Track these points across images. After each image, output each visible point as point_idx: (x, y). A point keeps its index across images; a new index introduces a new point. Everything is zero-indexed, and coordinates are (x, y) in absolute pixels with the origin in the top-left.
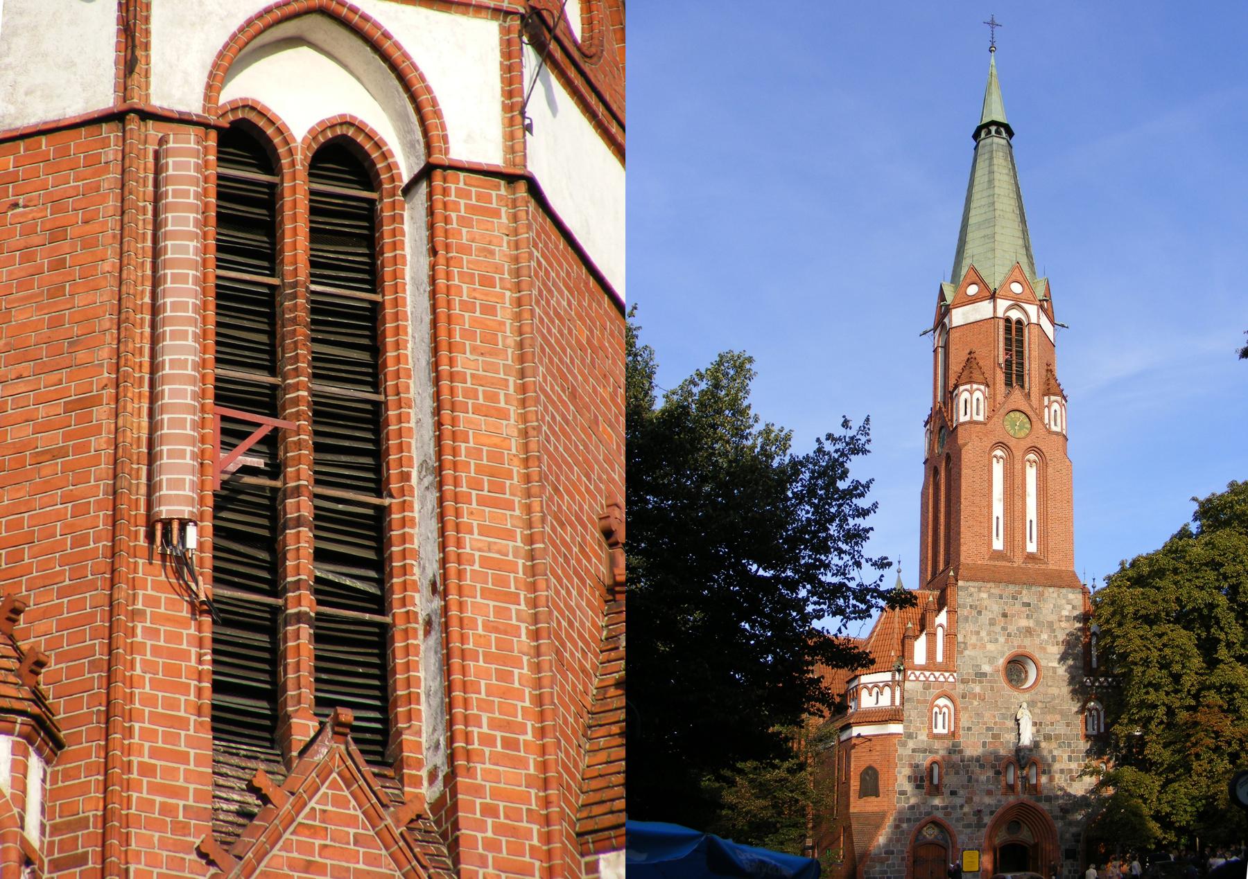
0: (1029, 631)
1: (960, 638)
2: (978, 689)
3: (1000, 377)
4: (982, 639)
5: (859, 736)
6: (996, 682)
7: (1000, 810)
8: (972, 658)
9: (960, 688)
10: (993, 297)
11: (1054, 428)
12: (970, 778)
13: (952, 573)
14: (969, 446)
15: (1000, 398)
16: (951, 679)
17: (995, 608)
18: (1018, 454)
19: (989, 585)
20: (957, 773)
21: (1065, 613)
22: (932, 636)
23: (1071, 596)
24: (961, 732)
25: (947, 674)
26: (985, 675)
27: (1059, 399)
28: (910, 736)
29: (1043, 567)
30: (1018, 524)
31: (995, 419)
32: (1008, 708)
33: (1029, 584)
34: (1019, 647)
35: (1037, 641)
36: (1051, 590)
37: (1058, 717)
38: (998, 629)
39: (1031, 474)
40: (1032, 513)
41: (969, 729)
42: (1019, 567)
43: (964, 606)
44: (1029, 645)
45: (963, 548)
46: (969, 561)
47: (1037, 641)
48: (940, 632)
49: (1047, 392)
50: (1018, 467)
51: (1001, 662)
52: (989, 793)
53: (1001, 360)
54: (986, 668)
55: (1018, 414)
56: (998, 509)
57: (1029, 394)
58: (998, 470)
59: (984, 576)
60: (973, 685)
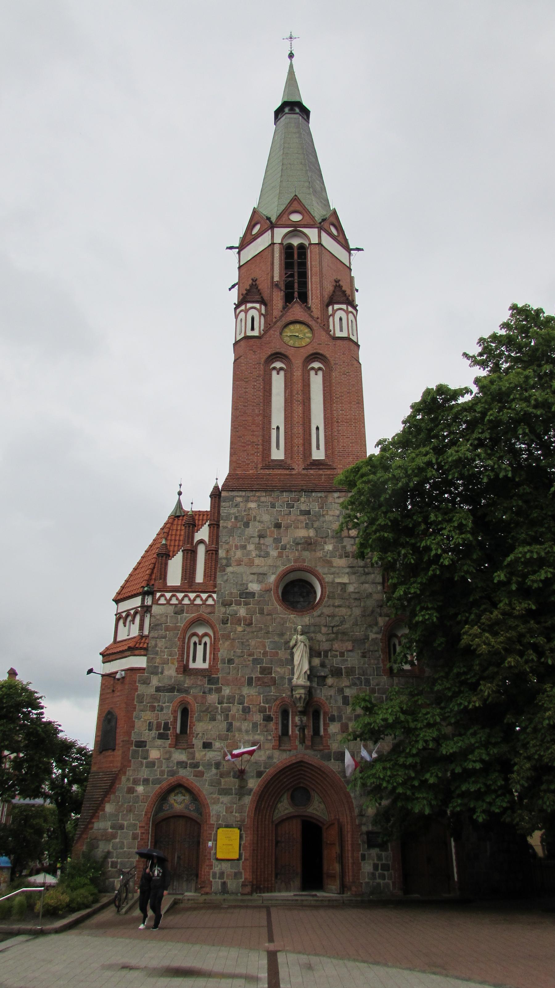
1: (222, 553)
2: (242, 612)
7: (270, 772)
9: (221, 611)
11: (338, 334)
12: (230, 727)
15: (276, 313)
19: (258, 494)
20: (213, 719)
24: (220, 666)
25: (204, 596)
26: (252, 594)
27: (344, 307)
31: (271, 332)
32: (282, 635)
35: (320, 554)
37: (349, 645)
38: (269, 541)
39: (317, 383)
41: (230, 661)
42: (299, 474)
43: (228, 518)
44: (309, 558)
47: (320, 554)
48: (201, 551)
50: (298, 374)
51: (272, 579)
54: (254, 587)
55: (298, 326)
56: (278, 418)
58: (278, 382)
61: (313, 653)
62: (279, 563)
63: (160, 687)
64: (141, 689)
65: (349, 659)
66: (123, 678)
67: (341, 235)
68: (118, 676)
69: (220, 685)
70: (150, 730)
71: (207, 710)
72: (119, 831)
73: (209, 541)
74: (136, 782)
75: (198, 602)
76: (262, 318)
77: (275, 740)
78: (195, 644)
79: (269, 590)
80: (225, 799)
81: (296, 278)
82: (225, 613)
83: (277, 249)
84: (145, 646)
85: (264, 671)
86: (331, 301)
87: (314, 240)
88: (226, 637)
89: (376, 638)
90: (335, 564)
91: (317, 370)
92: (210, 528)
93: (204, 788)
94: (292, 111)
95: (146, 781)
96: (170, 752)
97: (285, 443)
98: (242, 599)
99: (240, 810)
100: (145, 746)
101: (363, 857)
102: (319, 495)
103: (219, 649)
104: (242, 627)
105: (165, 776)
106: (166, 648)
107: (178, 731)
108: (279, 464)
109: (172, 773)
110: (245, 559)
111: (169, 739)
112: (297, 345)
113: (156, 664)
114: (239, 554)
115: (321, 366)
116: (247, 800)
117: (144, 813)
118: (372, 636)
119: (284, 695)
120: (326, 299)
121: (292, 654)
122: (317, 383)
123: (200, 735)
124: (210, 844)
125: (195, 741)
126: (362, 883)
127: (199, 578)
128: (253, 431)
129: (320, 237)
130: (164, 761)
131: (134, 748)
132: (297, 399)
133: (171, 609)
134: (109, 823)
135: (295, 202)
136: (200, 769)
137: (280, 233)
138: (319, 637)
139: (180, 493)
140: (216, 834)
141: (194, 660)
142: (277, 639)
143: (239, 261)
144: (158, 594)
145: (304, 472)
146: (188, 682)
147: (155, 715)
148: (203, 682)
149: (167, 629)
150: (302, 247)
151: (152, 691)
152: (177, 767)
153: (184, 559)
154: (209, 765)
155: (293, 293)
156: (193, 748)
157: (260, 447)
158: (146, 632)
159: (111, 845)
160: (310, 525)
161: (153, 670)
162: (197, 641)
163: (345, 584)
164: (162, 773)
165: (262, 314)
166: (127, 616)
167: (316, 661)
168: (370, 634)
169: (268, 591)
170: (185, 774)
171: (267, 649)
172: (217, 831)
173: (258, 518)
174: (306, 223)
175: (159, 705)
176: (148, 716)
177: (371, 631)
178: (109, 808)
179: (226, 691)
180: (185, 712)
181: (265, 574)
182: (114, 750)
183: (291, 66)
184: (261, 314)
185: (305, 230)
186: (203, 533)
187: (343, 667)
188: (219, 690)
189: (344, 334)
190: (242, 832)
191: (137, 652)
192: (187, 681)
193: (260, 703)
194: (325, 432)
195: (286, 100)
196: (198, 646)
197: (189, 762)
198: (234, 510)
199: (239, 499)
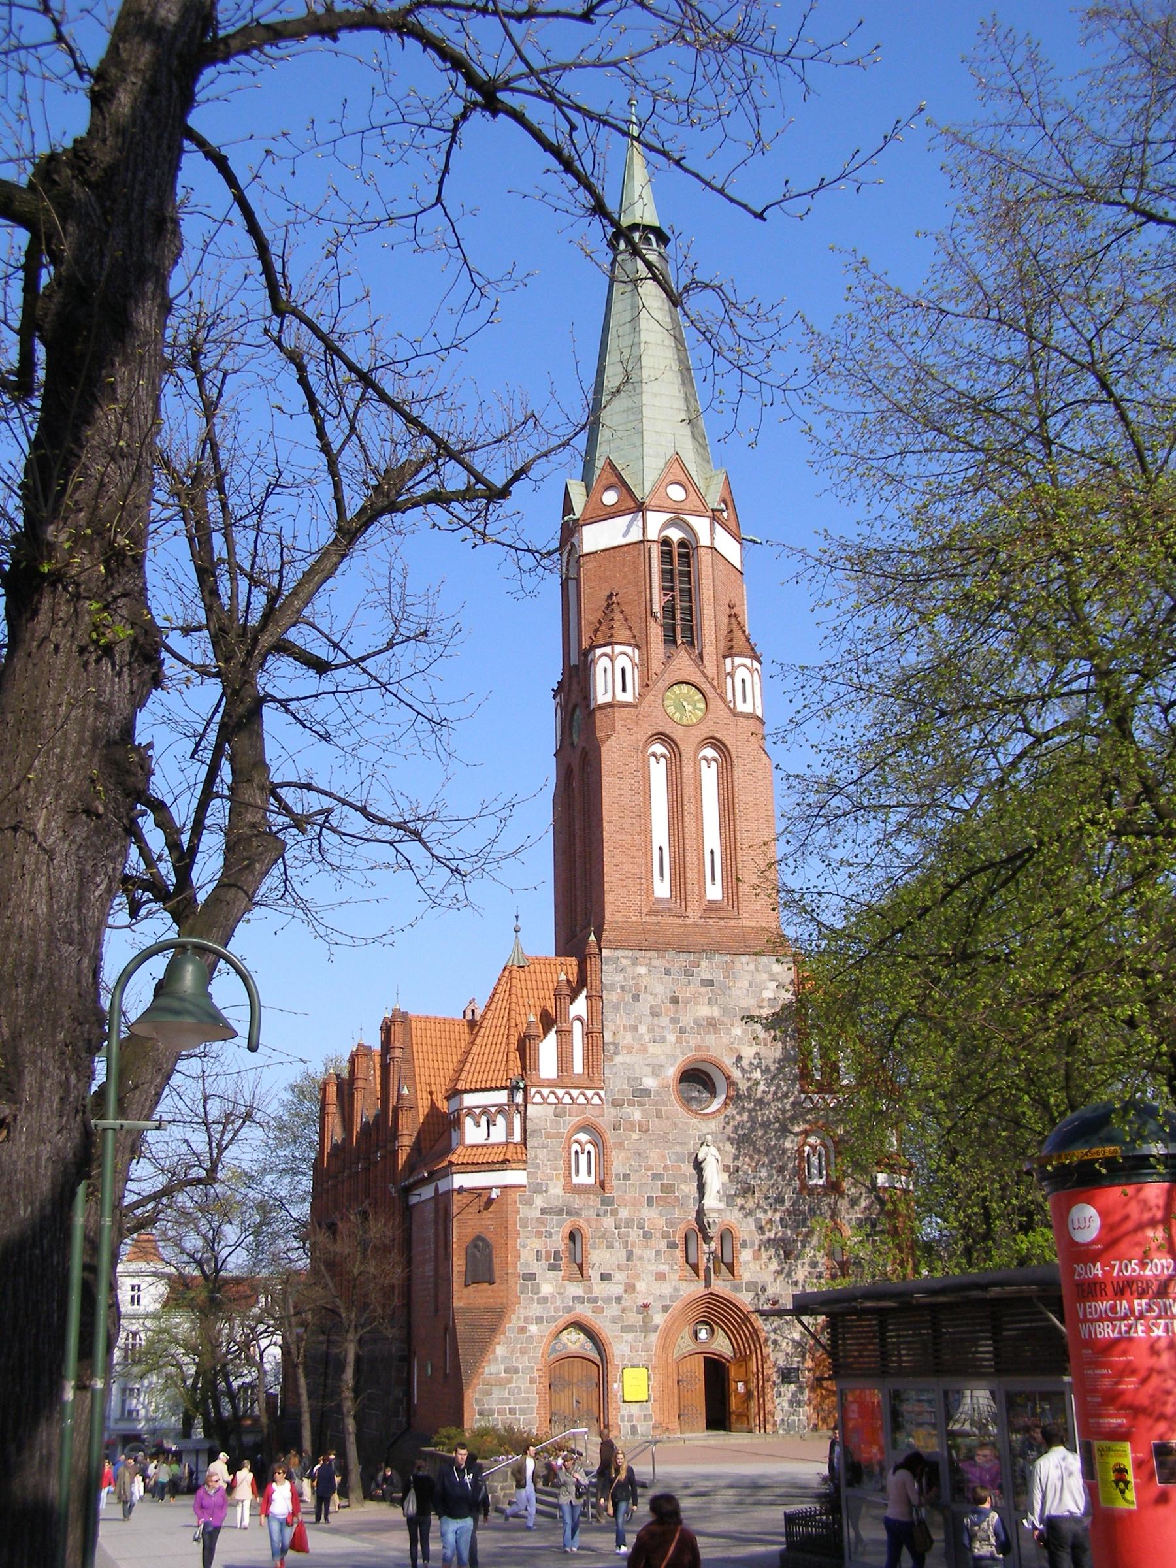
0: (712, 1025)
1: (608, 1037)
2: (637, 1115)
3: (656, 632)
5: (461, 1190)
6: (664, 1103)
7: (677, 1304)
8: (629, 1067)
9: (611, 1113)
10: (640, 508)
11: (741, 708)
13: (592, 938)
14: (612, 742)
15: (656, 666)
16: (596, 1100)
17: (661, 989)
18: (687, 749)
19: (649, 954)
20: (610, 1246)
21: (768, 994)
22: (564, 1036)
23: (777, 968)
24: (614, 1182)
25: (589, 1093)
26: (647, 1092)
27: (747, 661)
28: (538, 1189)
29: (732, 923)
30: (691, 858)
31: (650, 698)
33: (711, 949)
34: (698, 1048)
36: (744, 959)
38: (664, 1021)
39: (710, 777)
40: (712, 839)
41: (626, 1177)
43: (613, 987)
45: (608, 898)
46: (619, 918)
47: (726, 1039)
48: (577, 1028)
49: (729, 653)
50: (688, 769)
51: (672, 1072)
52: (661, 1277)
53: (657, 608)
54: (649, 1083)
55: (685, 688)
57: (701, 655)
59: (644, 942)
60: (629, 1110)
62: (678, 1052)
64: (524, 1211)
71: (603, 1236)
75: (582, 1100)
79: (668, 1087)
80: (630, 1337)
85: (667, 1188)
88: (620, 1145)
93: (604, 1326)
95: (539, 1320)
96: (564, 1287)
99: (647, 1349)
109: (568, 1310)
110: (637, 1045)
112: (685, 722)
114: (627, 1039)
125: (591, 1272)
127: (578, 1067)
134: (502, 1367)
142: (678, 1149)
144: (533, 1091)
146: (577, 1202)
148: (595, 1201)
150: (682, 544)
151: (538, 1214)
153: (560, 1044)
154: (608, 1300)
164: (556, 1310)
170: (584, 1312)
176: (536, 1244)
178: (500, 1350)
179: (624, 1213)
180: (572, 1237)
184: (634, 665)
188: (614, 1213)
191: (514, 1165)
198: (619, 978)
199: (624, 961)
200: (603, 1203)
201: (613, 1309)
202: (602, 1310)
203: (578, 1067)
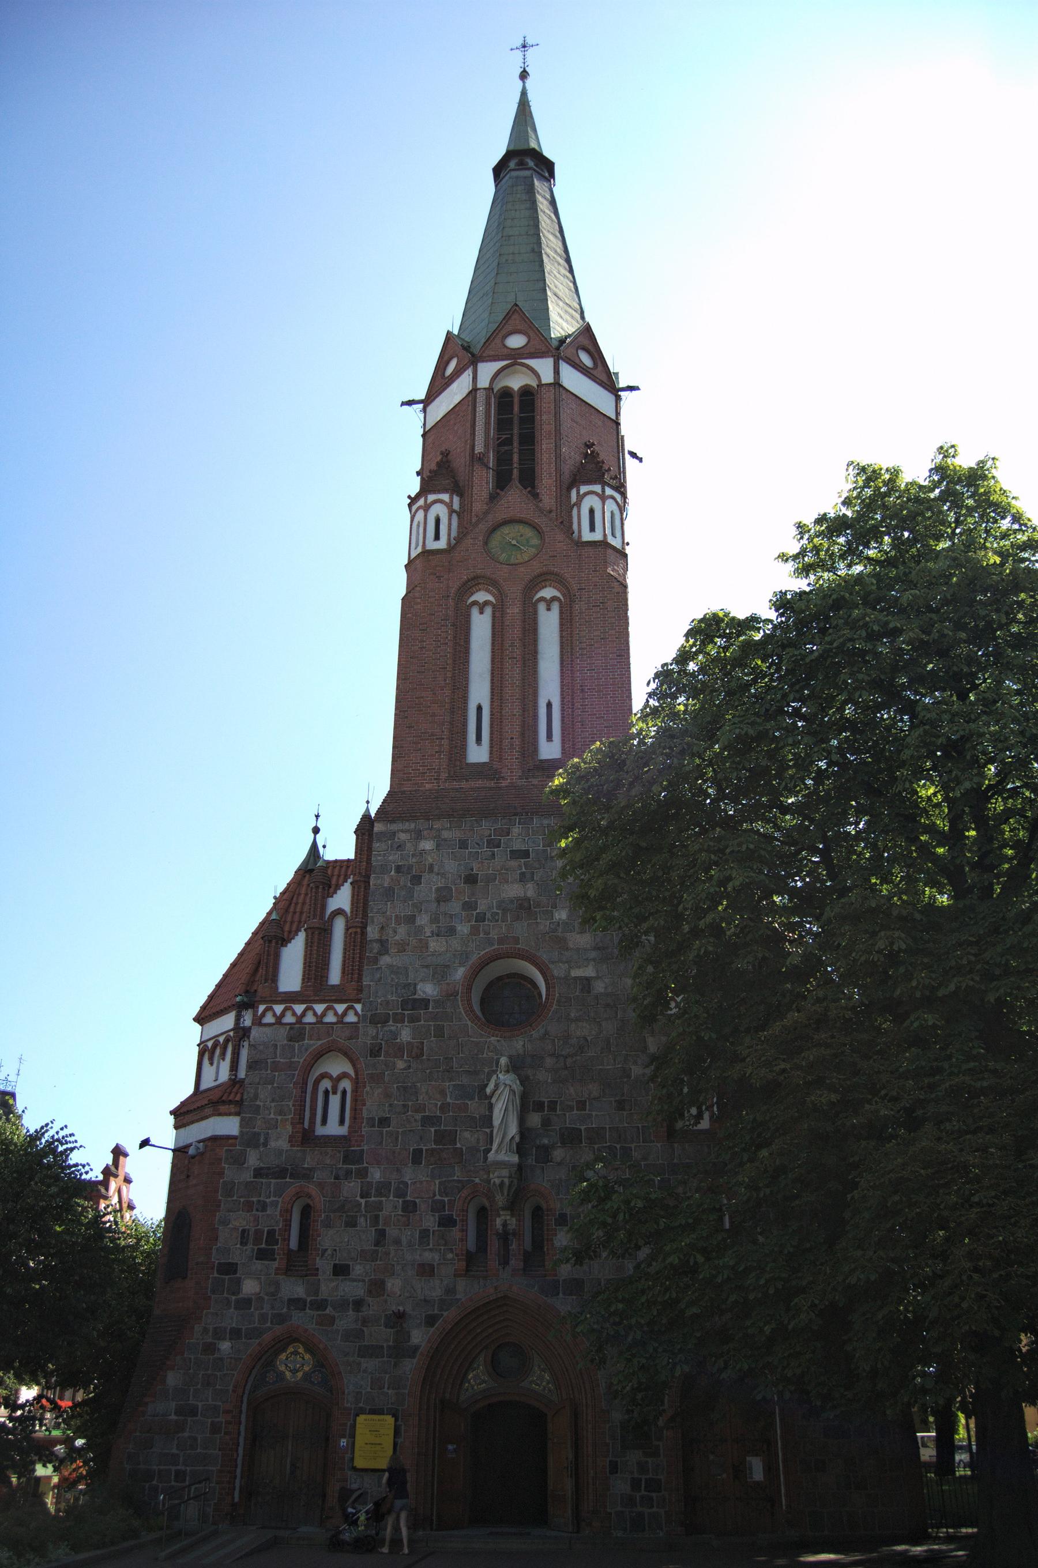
0: (524, 908)
1: (372, 932)
2: (406, 1035)
4: (420, 930)
9: (369, 1034)
11: (587, 536)
15: (478, 507)
20: (352, 1223)
24: (365, 1130)
25: (340, 1008)
26: (425, 1003)
27: (597, 488)
31: (468, 541)
34: (501, 941)
38: (455, 907)
39: (549, 623)
41: (384, 1122)
43: (384, 869)
48: (339, 927)
51: (460, 973)
52: (426, 1270)
54: (428, 989)
56: (479, 692)
58: (481, 626)
61: (526, 1104)
63: (261, 1168)
65: (594, 1113)
66: (202, 1154)
67: (600, 367)
68: (192, 1151)
69: (365, 1165)
70: (244, 1243)
72: (189, 1419)
73: (352, 912)
74: (219, 1334)
75: (330, 1018)
76: (455, 517)
77: (459, 1260)
78: (326, 1093)
79: (455, 994)
80: (370, 1364)
81: (516, 444)
82: (375, 1037)
83: (481, 397)
84: (238, 1098)
85: (441, 1137)
86: (575, 481)
87: (547, 377)
89: (644, 1075)
90: (571, 945)
91: (549, 603)
92: (354, 888)
94: (522, 165)
95: (235, 1334)
97: (492, 733)
98: (406, 1012)
100: (235, 1272)
101: (614, 1468)
102: (546, 822)
103: (364, 1100)
104: (406, 1061)
105: (269, 1324)
106: (273, 1101)
107: (294, 1244)
108: (480, 769)
109: (280, 1319)
111: (275, 1260)
112: (512, 561)
113: (256, 1130)
115: (558, 594)
116: (409, 1366)
117: (231, 1388)
118: (636, 1070)
119: (477, 1180)
120: (567, 476)
121: (491, 1107)
122: (549, 623)
123: (329, 1252)
124: (343, 1442)
126: (610, 1514)
127: (335, 977)
128: (434, 715)
129: (557, 372)
130: (266, 1298)
131: (216, 1275)
132: (516, 652)
133: (283, 1032)
134: (173, 1404)
135: (516, 316)
136: (327, 1311)
137: (487, 370)
138: (542, 1076)
139: (316, 830)
140: (354, 1426)
141: (324, 1122)
143: (424, 425)
144: (262, 1008)
145: (522, 782)
147: (252, 1219)
149: (276, 1067)
150: (527, 392)
151: (248, 1176)
152: (289, 1308)
153: (309, 945)
154: (342, 1305)
155: (511, 471)
156: (317, 1275)
157: (445, 742)
158: (242, 1074)
159: (176, 1442)
160: (528, 876)
161: (250, 1139)
162: (330, 1089)
163: (588, 979)
165: (454, 511)
166: (215, 1046)
167: (535, 1120)
168: (633, 1067)
169: (452, 995)
170: (303, 1320)
171: (448, 1100)
172: (355, 1421)
173: (436, 869)
174: (532, 350)
175: (259, 1201)
176: (240, 1220)
177: (635, 1063)
178: (173, 1379)
179: (376, 1175)
180: (306, 1212)
181: (448, 966)
182: (184, 1278)
183: (524, 93)
184: (451, 511)
185: (531, 362)
186: (342, 899)
187: (583, 1128)
188: (363, 1173)
189: (597, 536)
190: (399, 1423)
191: (223, 1108)
192: (308, 1159)
193: (435, 1195)
194: (563, 710)
195: (512, 148)
196: (332, 1097)
197: (309, 1299)
198: (394, 857)
199: (403, 836)
200: (346, 1159)
201: (347, 1321)
202: (332, 1320)
203: (335, 977)
